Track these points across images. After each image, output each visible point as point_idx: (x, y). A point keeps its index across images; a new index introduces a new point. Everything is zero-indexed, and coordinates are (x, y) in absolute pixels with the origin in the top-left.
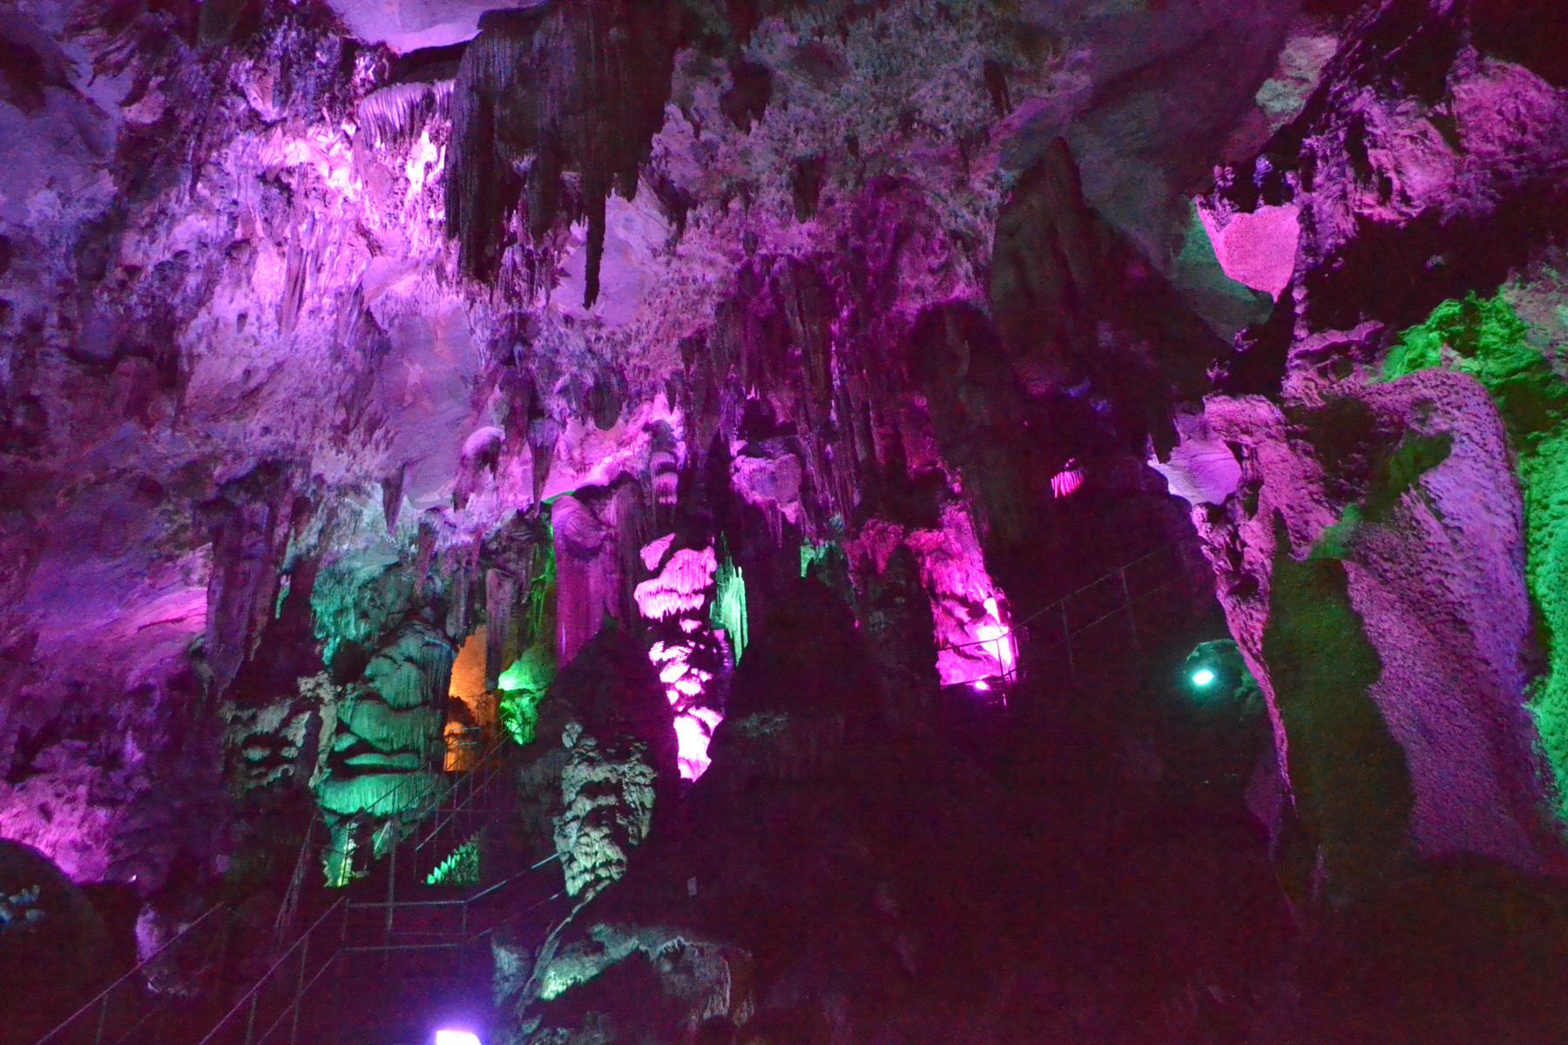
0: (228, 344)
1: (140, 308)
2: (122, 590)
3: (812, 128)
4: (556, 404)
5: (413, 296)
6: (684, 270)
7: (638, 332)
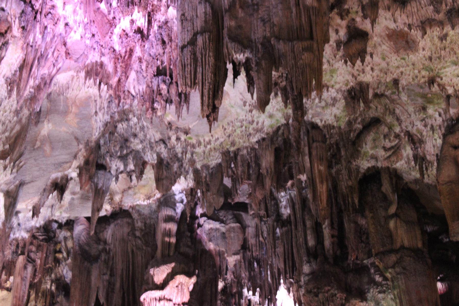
3: (381, 71)
7: (209, 143)
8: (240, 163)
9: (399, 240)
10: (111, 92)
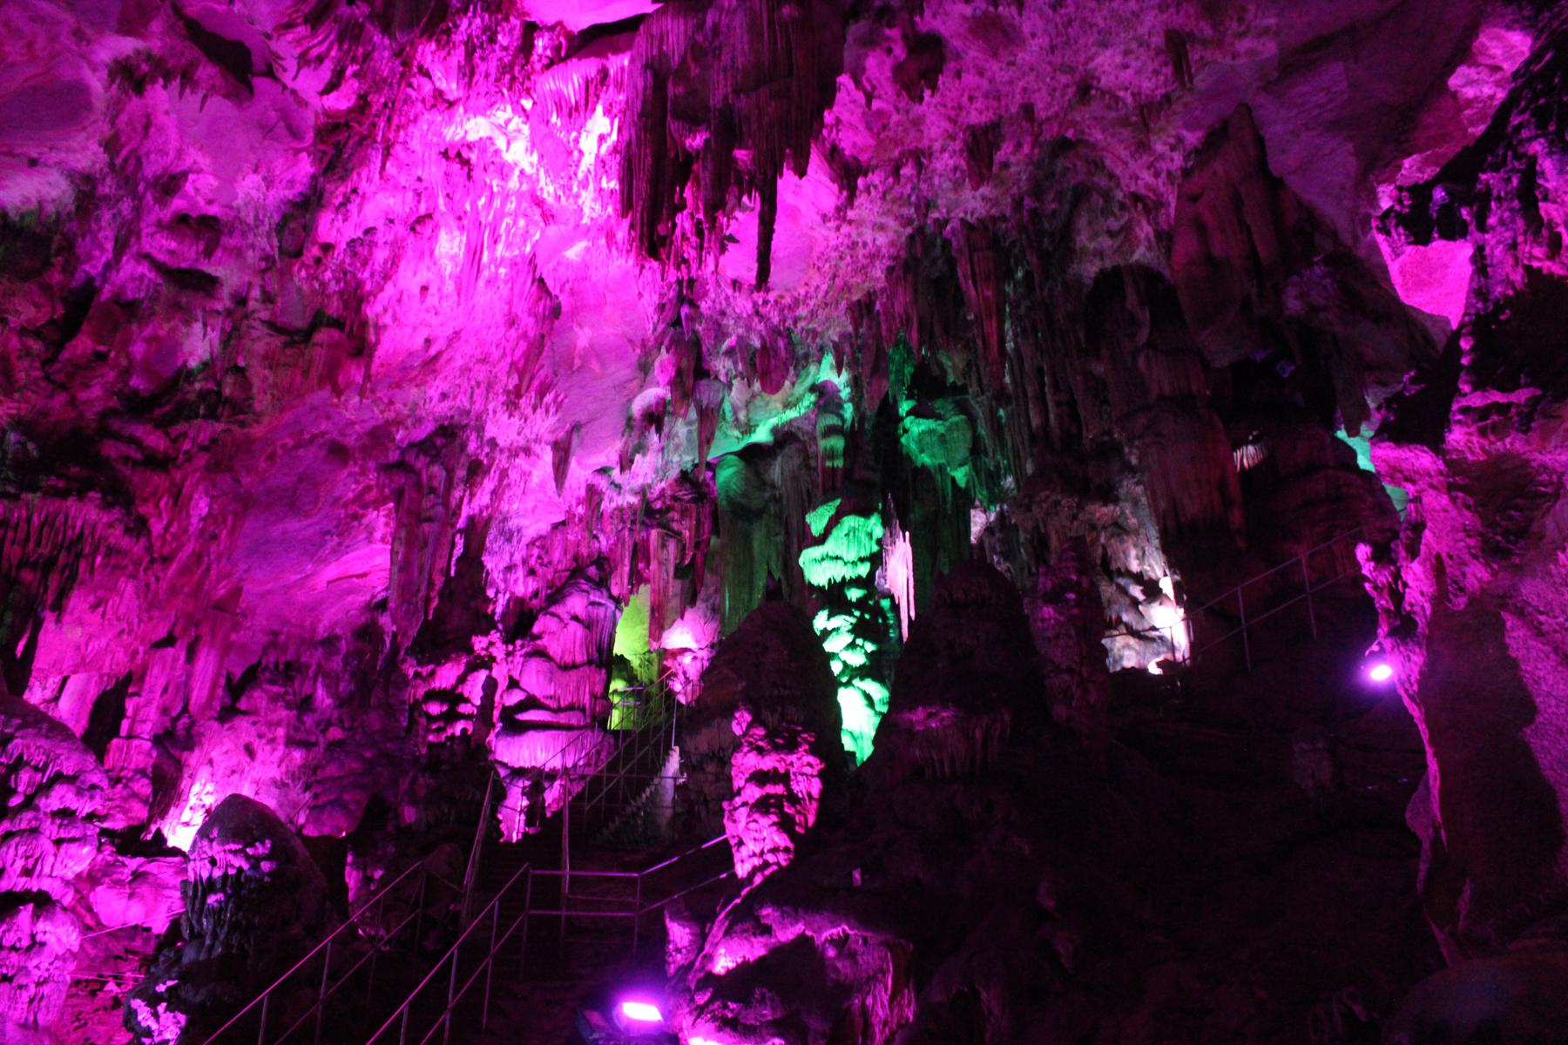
1: (333, 283)
2: (313, 549)
3: (986, 96)
4: (722, 365)
6: (854, 235)
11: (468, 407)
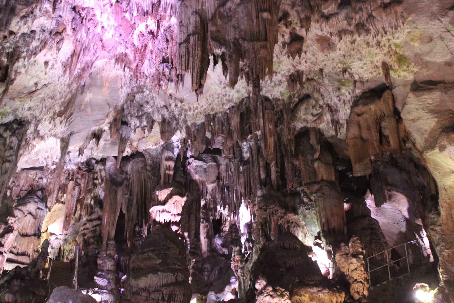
0: (33, 71)
3: (312, 63)
4: (134, 122)
5: (103, 67)
7: (197, 108)
8: (217, 123)
9: (320, 175)
10: (132, 73)
11: (38, 115)
